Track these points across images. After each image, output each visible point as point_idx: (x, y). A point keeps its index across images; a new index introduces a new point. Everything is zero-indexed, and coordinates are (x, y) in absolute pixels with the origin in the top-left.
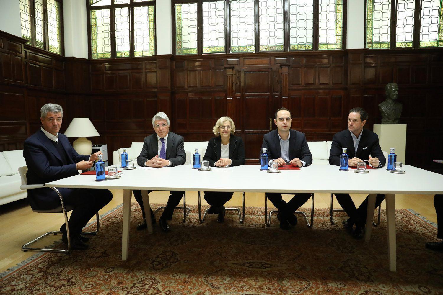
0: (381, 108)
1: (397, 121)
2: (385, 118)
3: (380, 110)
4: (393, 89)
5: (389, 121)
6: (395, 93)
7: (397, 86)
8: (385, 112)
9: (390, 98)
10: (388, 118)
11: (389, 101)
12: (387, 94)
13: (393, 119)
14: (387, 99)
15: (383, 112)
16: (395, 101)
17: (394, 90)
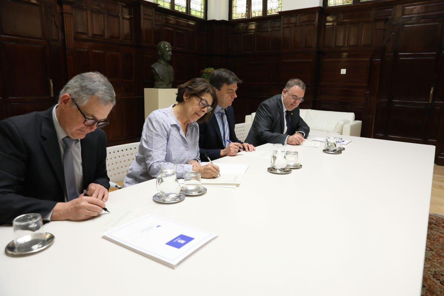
0: (155, 70)
1: (171, 85)
2: (159, 82)
3: (154, 71)
4: (167, 49)
5: (163, 85)
6: (169, 53)
7: (170, 46)
8: (159, 74)
9: (164, 60)
10: (162, 82)
11: (162, 62)
12: (160, 54)
13: (168, 83)
14: (159, 60)
15: (157, 74)
16: (170, 63)
17: (168, 50)
